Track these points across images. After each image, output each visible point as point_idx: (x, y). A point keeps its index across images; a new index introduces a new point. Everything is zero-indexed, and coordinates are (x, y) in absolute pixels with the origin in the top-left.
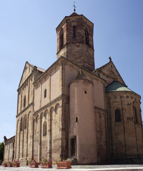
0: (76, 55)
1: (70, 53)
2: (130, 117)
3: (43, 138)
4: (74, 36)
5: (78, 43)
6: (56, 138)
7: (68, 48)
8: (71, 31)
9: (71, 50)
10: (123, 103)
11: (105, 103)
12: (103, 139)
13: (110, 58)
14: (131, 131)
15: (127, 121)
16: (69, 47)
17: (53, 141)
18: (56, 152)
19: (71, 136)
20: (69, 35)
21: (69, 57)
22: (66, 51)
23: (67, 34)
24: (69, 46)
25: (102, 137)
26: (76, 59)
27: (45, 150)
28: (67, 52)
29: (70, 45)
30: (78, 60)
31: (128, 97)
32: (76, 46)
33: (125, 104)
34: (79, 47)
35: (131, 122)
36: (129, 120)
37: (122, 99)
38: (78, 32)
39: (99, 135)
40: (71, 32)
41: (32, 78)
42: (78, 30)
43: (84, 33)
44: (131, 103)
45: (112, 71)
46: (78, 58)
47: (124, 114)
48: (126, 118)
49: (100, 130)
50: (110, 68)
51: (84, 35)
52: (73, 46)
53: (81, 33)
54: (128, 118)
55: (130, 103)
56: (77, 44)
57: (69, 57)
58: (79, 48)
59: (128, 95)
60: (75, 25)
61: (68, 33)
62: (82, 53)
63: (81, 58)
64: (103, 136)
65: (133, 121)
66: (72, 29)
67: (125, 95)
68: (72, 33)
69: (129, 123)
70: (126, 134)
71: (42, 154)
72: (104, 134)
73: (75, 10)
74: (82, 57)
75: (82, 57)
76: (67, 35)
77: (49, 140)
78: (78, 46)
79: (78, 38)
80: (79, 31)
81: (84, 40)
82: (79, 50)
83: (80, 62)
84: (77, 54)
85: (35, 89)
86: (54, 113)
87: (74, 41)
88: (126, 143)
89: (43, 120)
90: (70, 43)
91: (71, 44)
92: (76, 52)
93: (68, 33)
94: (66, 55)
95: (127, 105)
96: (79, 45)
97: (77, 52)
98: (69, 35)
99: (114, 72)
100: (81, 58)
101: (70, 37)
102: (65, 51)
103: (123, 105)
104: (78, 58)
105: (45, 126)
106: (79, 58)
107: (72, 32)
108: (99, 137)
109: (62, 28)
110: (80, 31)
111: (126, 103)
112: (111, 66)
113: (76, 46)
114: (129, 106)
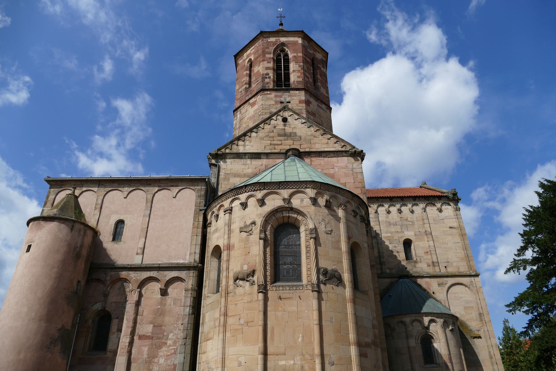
1: (239, 128)
2: (245, 267)
11: (194, 242)
12: (162, 361)
14: (242, 321)
25: (161, 354)
35: (244, 287)
37: (227, 215)
39: (145, 349)
43: (267, 68)
44: (254, 223)
45: (285, 135)
48: (231, 275)
49: (152, 333)
50: (275, 127)
51: (265, 72)
55: (248, 223)
58: (256, 107)
59: (243, 197)
62: (260, 115)
64: (164, 349)
65: (253, 284)
68: (244, 83)
69: (239, 290)
72: (169, 342)
78: (253, 105)
81: (268, 83)
87: (247, 98)
98: (240, 90)
99: (294, 131)
101: (241, 92)
107: (247, 79)
108: (145, 356)
112: (285, 120)
114: (244, 234)
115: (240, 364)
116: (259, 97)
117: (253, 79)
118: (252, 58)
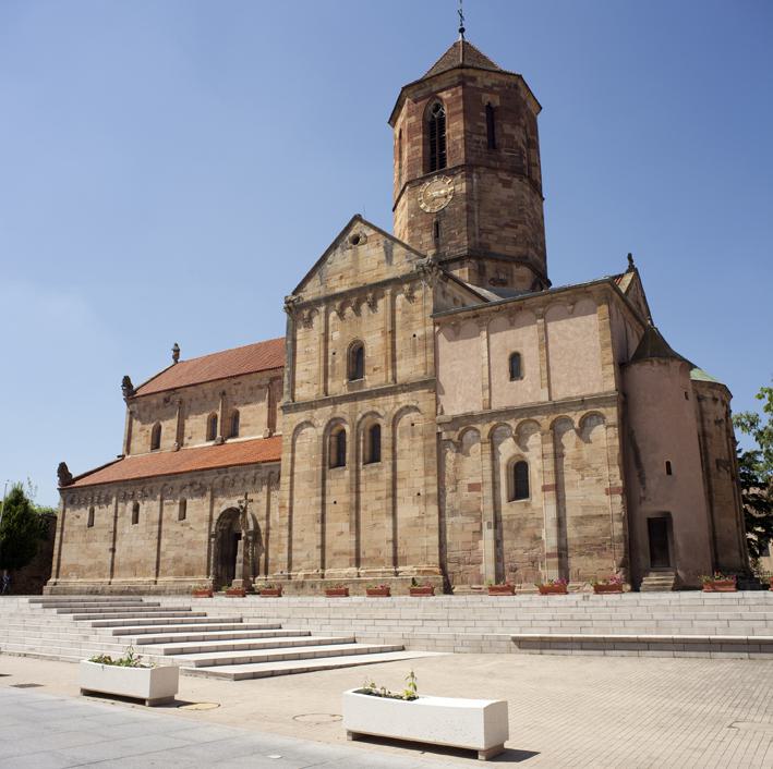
0: (502, 212)
1: (480, 200)
3: (511, 506)
4: (492, 144)
5: (506, 171)
6: (587, 513)
7: (472, 182)
8: (480, 124)
9: (482, 191)
10: (705, 416)
13: (630, 257)
15: (716, 471)
16: (475, 180)
17: (569, 521)
18: (590, 555)
19: (650, 509)
20: (476, 137)
21: (476, 216)
22: (462, 187)
23: (465, 131)
24: (474, 175)
26: (502, 227)
27: (528, 545)
28: (469, 195)
29: (478, 173)
30: (508, 233)
31: (715, 400)
32: (501, 180)
33: (709, 421)
34: (510, 187)
36: (722, 469)
38: (506, 131)
40: (482, 127)
41: (412, 290)
42: (504, 126)
46: (507, 225)
47: (709, 450)
52: (488, 178)
53: (516, 137)
54: (718, 462)
56: (503, 176)
57: (476, 216)
58: (511, 192)
59: (717, 393)
60: (494, 105)
61: (468, 128)
62: (521, 211)
63: (516, 227)
66: (483, 114)
67: (708, 395)
68: (482, 132)
69: (721, 475)
70: (716, 509)
71: (506, 558)
73: (462, 30)
74: (519, 226)
75: (519, 226)
76: (468, 135)
77: (550, 513)
78: (507, 184)
79: (505, 154)
80: (507, 129)
82: (509, 197)
83: (515, 242)
84: (504, 212)
85: (441, 337)
86: (569, 439)
87: (492, 163)
88: (718, 534)
89: (507, 449)
90: (477, 166)
91: (482, 170)
92: (499, 203)
93: (468, 128)
94: (464, 204)
95: (712, 422)
96: (511, 182)
97: (504, 204)
98: (476, 137)
100: (516, 227)
101: (478, 142)
102: (458, 188)
103: (706, 423)
104: (507, 225)
105: (520, 471)
106: (513, 227)
107: (485, 125)
109: (441, 100)
110: (514, 132)
111: (712, 417)
113: (501, 180)
115: (729, 531)
116: (516, 180)
117: (499, 140)
118: (497, 102)
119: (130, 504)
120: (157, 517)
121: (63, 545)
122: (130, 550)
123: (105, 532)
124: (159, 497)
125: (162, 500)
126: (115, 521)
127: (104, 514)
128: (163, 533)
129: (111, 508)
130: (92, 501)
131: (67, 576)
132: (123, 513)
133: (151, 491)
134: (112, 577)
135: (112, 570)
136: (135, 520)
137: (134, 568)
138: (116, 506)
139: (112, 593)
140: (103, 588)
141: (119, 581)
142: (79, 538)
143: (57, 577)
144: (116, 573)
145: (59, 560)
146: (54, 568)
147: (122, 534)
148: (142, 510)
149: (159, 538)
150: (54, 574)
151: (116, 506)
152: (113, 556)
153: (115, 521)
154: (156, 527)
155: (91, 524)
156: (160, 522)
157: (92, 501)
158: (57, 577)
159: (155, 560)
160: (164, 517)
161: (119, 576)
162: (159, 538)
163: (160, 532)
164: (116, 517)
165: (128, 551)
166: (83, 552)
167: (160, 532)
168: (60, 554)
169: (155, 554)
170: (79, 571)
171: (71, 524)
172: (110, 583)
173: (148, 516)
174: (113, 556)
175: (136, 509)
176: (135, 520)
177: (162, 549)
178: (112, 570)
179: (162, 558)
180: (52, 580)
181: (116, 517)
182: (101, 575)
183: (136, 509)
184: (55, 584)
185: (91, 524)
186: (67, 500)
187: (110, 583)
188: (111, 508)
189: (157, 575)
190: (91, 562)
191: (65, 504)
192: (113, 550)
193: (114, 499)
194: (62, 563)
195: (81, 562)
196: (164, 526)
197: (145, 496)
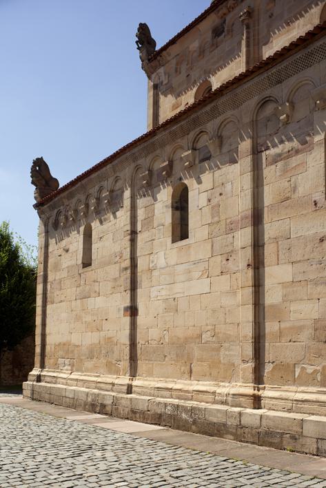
119: (165, 195)
120: (243, 204)
121: (49, 307)
122: (172, 306)
123: (113, 271)
124: (246, 145)
125: (256, 152)
126: (133, 241)
127: (110, 233)
128: (269, 251)
129: (123, 215)
130: (86, 215)
131: (56, 366)
132: (149, 220)
133: (220, 140)
134: (133, 373)
135: (133, 358)
136: (181, 231)
137: (184, 355)
138: (133, 208)
139: (134, 414)
140: (115, 401)
141: (151, 384)
142: (70, 291)
143: (42, 366)
144: (142, 365)
145: (44, 336)
146: (38, 350)
147: (150, 270)
148: (197, 199)
149: (257, 264)
150: (37, 359)
151: (133, 208)
152: (133, 326)
153: (133, 241)
154: (244, 237)
155: (87, 263)
156: (257, 218)
157: (86, 215)
158: (42, 366)
159: (248, 331)
160: (268, 199)
161: (150, 374)
162: (257, 264)
163: (258, 245)
164: (133, 233)
165: (167, 310)
166: (78, 318)
167: (258, 245)
168: (44, 325)
169: (247, 314)
170: (68, 349)
171: (57, 267)
172: (130, 390)
173: (216, 209)
174: (133, 326)
175: (181, 204)
176: (181, 231)
177: (272, 297)
178: (133, 358)
179: (271, 327)
180: (35, 372)
181: (133, 233)
182: (111, 368)
183: (181, 204)
184: (39, 379)
185: (87, 263)
186: (52, 220)
187: (130, 390)
188: (123, 215)
189: (258, 379)
190: (91, 338)
191: (47, 232)
192: (133, 311)
193: (127, 194)
194: (49, 340)
195: (75, 339)
196: (270, 229)
197: (203, 159)
